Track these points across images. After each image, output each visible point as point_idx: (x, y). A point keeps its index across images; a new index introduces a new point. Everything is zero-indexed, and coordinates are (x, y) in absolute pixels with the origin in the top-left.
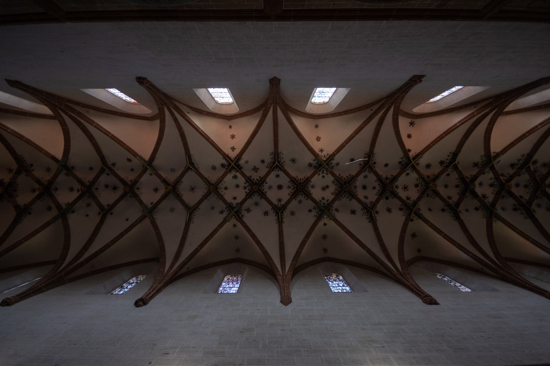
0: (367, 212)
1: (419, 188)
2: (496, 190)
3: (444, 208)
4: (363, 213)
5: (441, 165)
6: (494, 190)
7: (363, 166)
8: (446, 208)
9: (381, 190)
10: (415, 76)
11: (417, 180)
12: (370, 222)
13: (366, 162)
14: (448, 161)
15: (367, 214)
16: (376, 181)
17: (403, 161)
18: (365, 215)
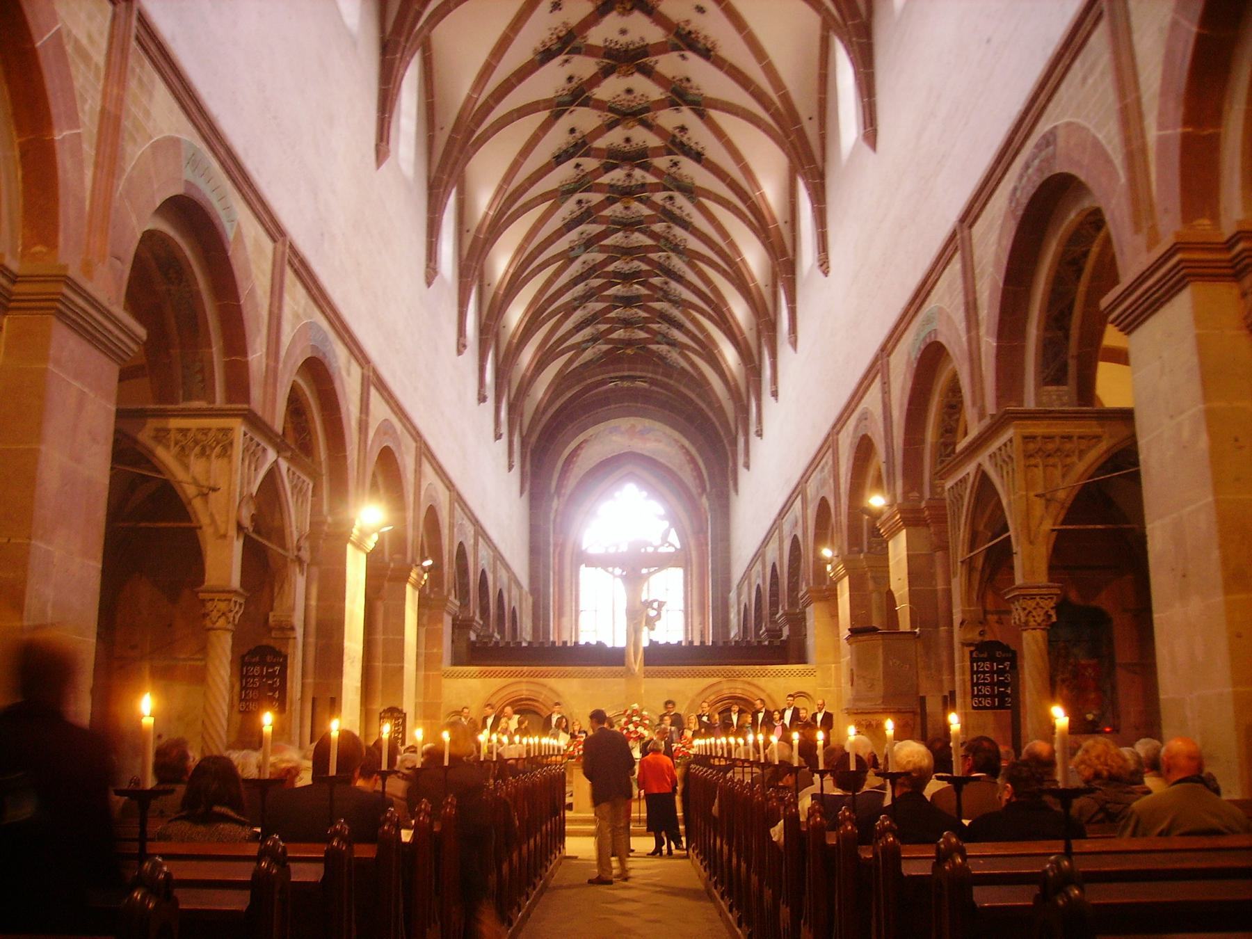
0: (559, 38)
1: (624, 96)
2: (620, 183)
3: (577, 131)
4: (556, 29)
5: (677, 128)
6: (619, 180)
7: (684, 29)
8: (578, 134)
9: (618, 47)
10: (828, 272)
11: (643, 95)
12: (536, 52)
13: (693, 36)
14: (685, 139)
15: (555, 36)
16: (642, 39)
17: (691, 88)
18: (552, 34)
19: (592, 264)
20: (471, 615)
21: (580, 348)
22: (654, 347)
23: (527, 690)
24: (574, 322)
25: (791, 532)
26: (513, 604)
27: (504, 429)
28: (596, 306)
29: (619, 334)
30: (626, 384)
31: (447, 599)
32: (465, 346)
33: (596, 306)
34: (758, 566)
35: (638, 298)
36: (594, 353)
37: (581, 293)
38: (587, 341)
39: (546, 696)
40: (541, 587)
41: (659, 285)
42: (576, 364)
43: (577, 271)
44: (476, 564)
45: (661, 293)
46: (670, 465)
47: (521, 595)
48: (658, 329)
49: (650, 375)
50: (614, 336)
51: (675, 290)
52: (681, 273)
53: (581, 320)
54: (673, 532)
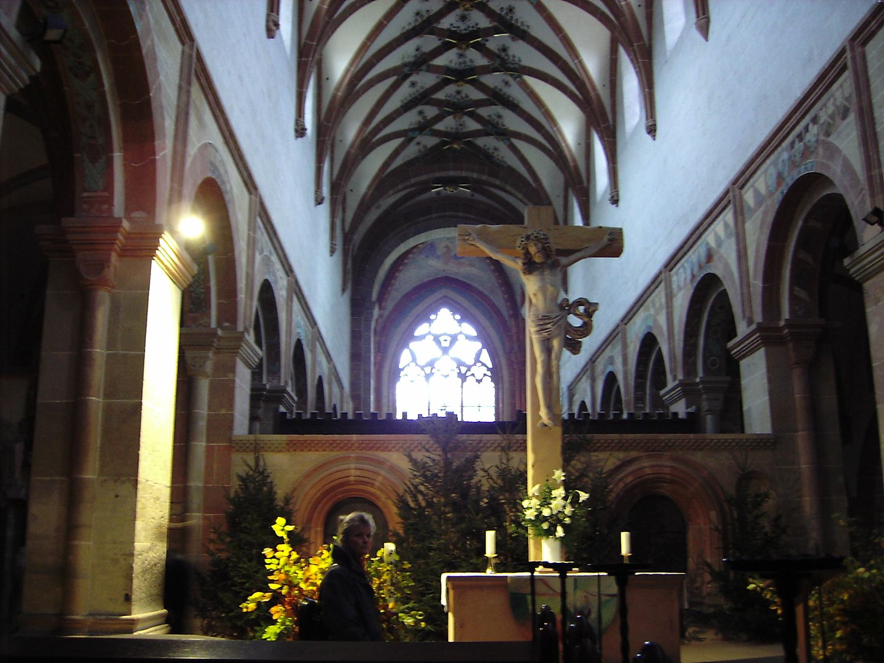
19: (426, 16)
20: (282, 384)
21: (407, 136)
22: (481, 142)
23: (356, 469)
24: (402, 101)
25: (693, 276)
26: (334, 402)
27: (326, 191)
28: (425, 80)
29: (448, 124)
30: (449, 191)
31: (241, 338)
32: (277, 25)
33: (425, 80)
34: (615, 351)
35: (473, 70)
36: (420, 151)
37: (411, 59)
38: (413, 130)
39: (384, 477)
40: (362, 394)
41: (496, 51)
42: (398, 162)
43: (410, 24)
44: (289, 333)
45: (498, 62)
46: (481, 289)
47: (342, 396)
48: (487, 118)
49: (475, 175)
50: (440, 126)
51: (514, 57)
52: (525, 28)
53: (409, 98)
54: (485, 351)
